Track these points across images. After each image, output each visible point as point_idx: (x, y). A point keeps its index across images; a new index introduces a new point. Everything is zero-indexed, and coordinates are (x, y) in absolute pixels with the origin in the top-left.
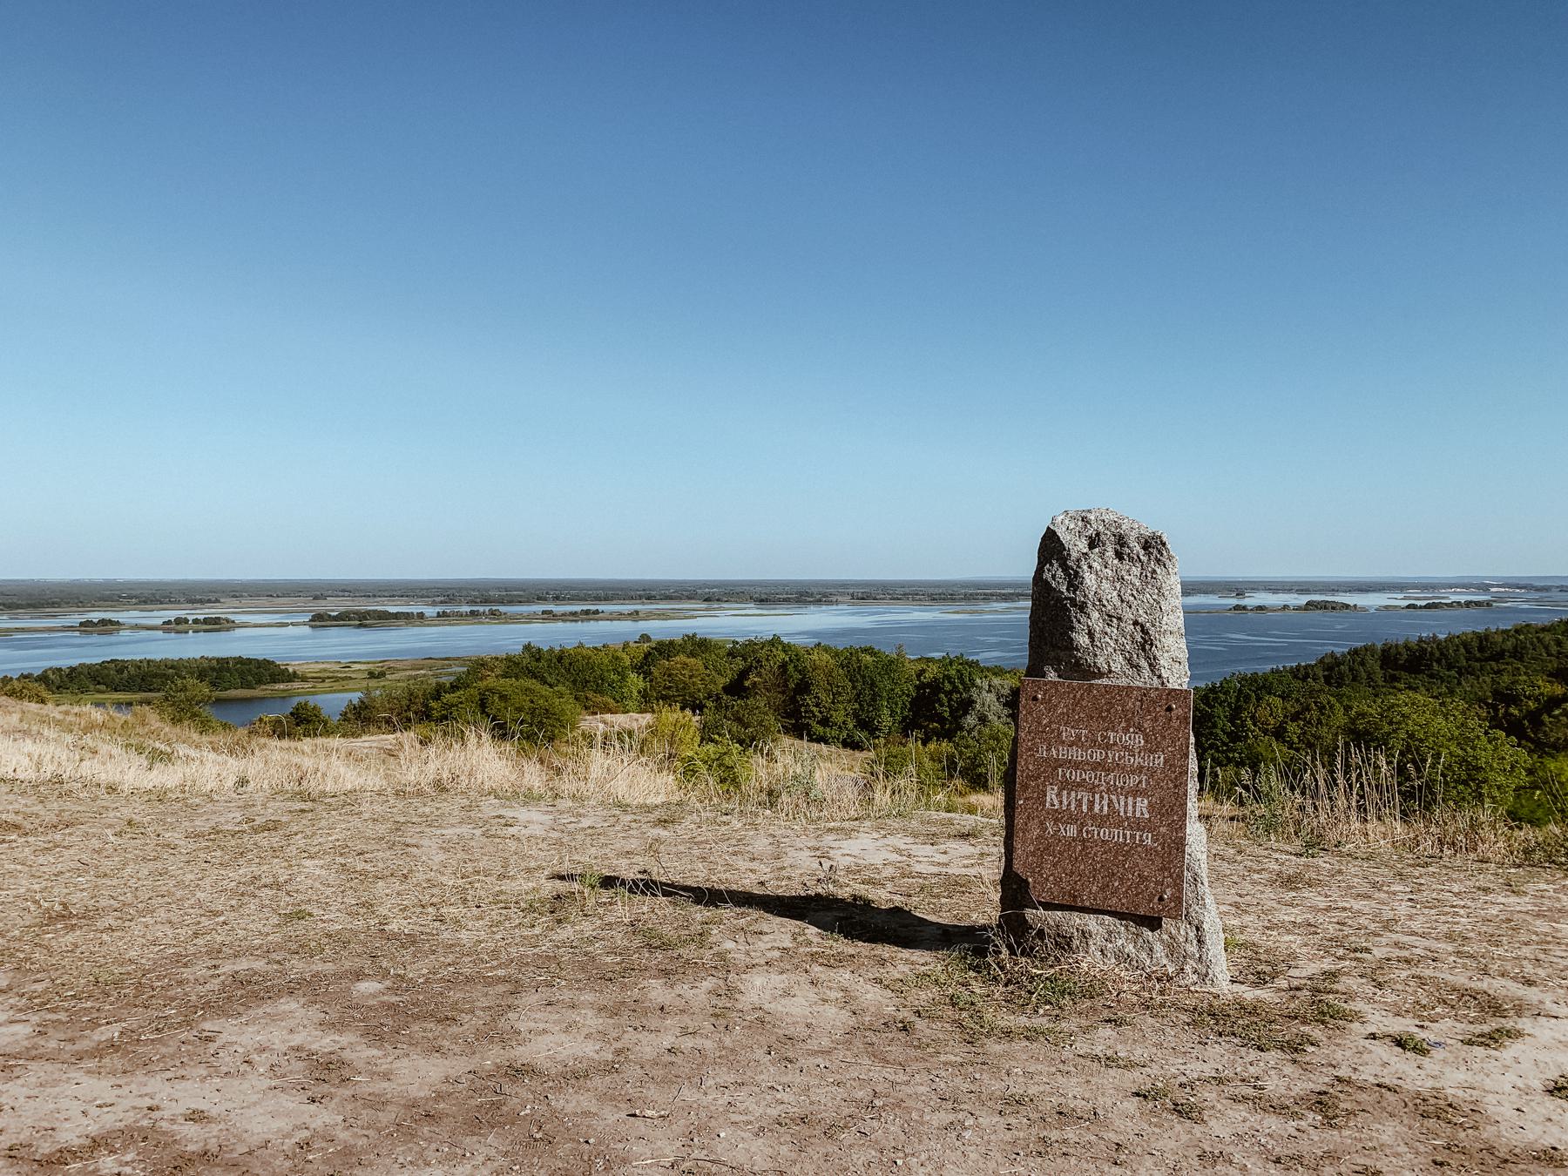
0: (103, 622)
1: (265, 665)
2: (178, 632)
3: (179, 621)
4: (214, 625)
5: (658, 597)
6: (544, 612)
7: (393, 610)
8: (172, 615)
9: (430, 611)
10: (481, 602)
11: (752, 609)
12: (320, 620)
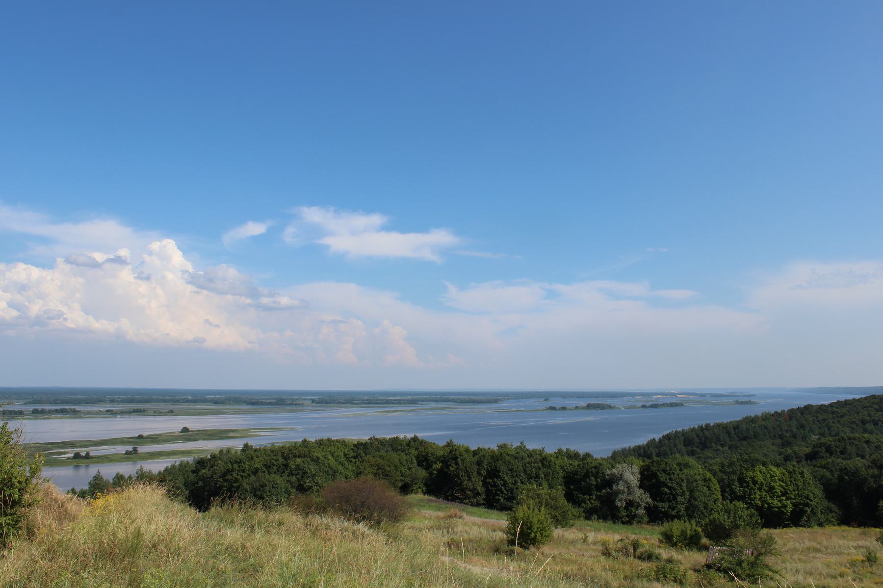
5: (182, 401)
6: (107, 411)
9: (31, 408)
10: (61, 403)
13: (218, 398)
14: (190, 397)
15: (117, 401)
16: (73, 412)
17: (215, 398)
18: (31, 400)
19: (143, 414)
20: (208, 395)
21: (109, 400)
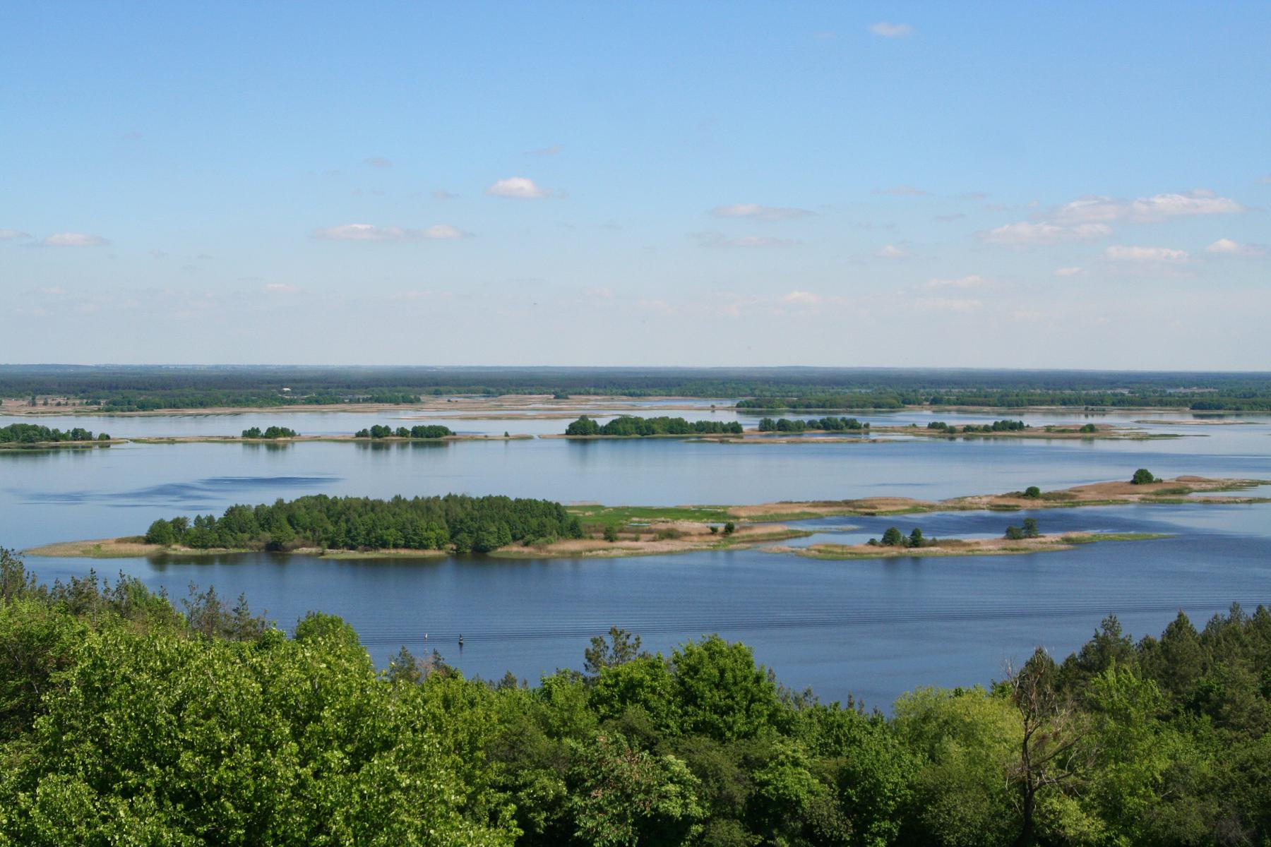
0: (273, 432)
1: (553, 511)
2: (377, 447)
3: (378, 432)
4: (431, 438)
7: (692, 418)
8: (367, 419)
11: (1185, 421)
12: (581, 433)
13: (1202, 395)
14: (1126, 392)
15: (949, 403)
16: (852, 427)
17: (1193, 394)
18: (748, 398)
19: (1016, 433)
20: (1170, 386)
21: (926, 400)
